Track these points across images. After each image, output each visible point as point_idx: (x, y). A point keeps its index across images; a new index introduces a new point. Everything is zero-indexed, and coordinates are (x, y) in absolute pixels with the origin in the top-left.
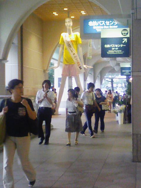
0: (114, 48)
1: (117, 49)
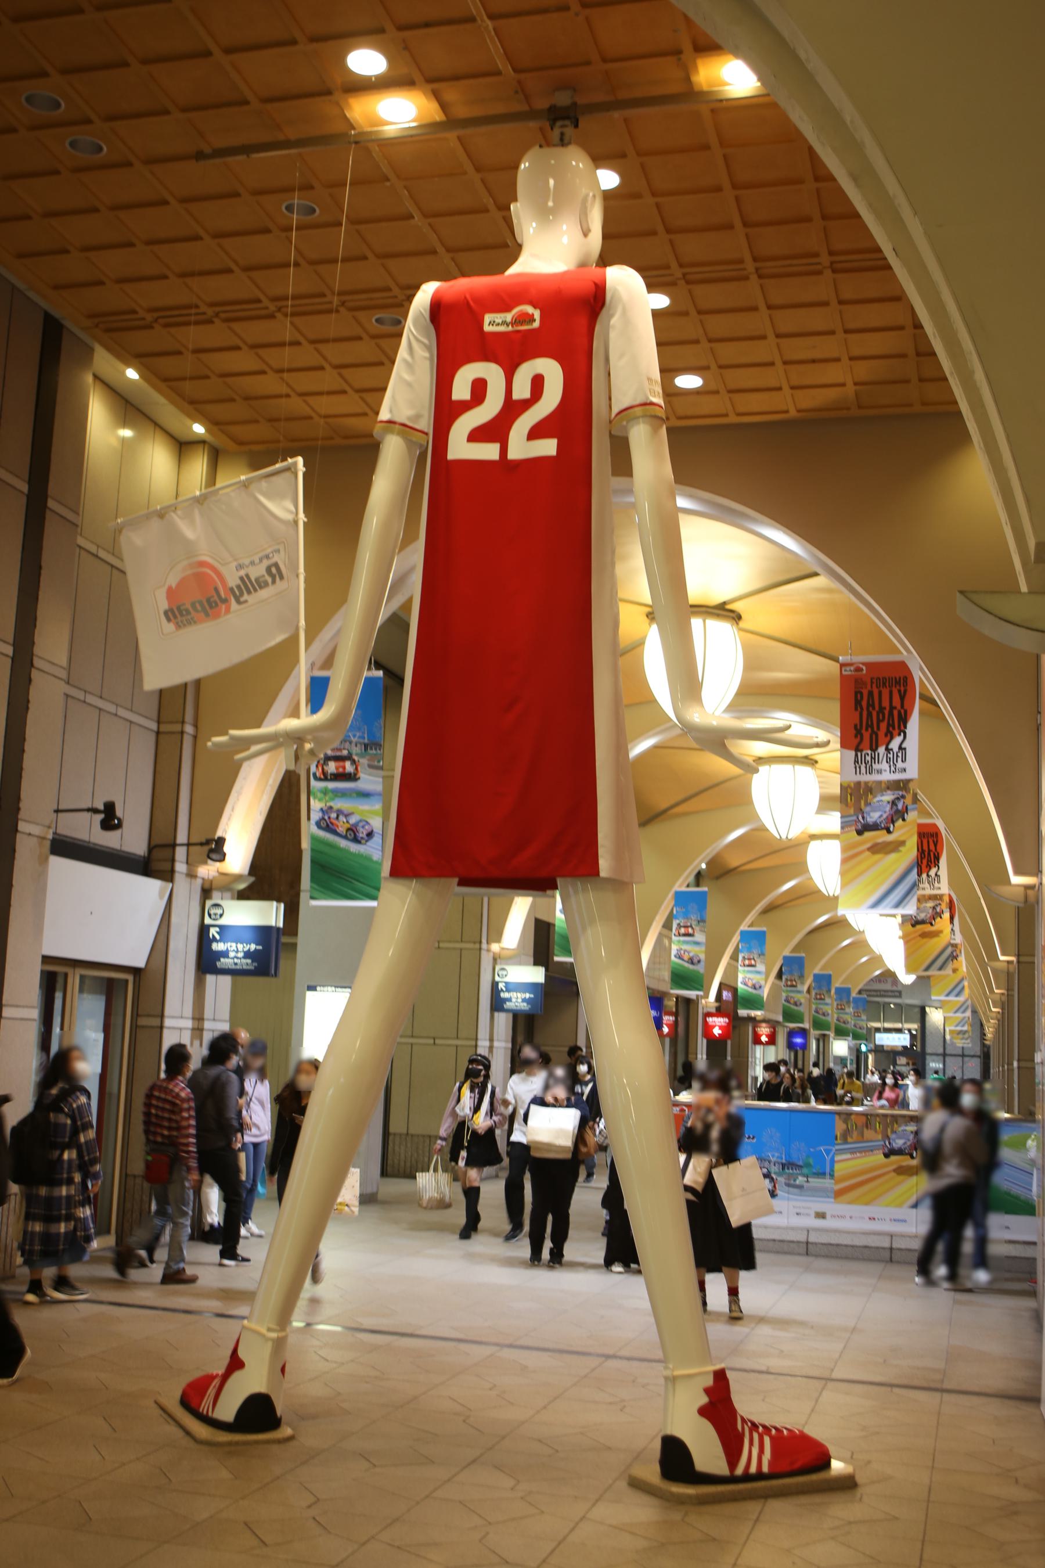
0: (234, 952)
1: (241, 955)
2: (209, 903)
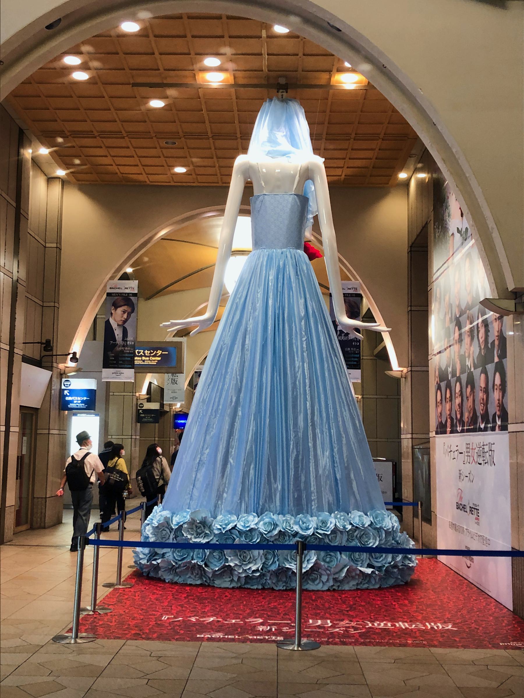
0: (76, 401)
1: (79, 402)
2: (63, 380)
